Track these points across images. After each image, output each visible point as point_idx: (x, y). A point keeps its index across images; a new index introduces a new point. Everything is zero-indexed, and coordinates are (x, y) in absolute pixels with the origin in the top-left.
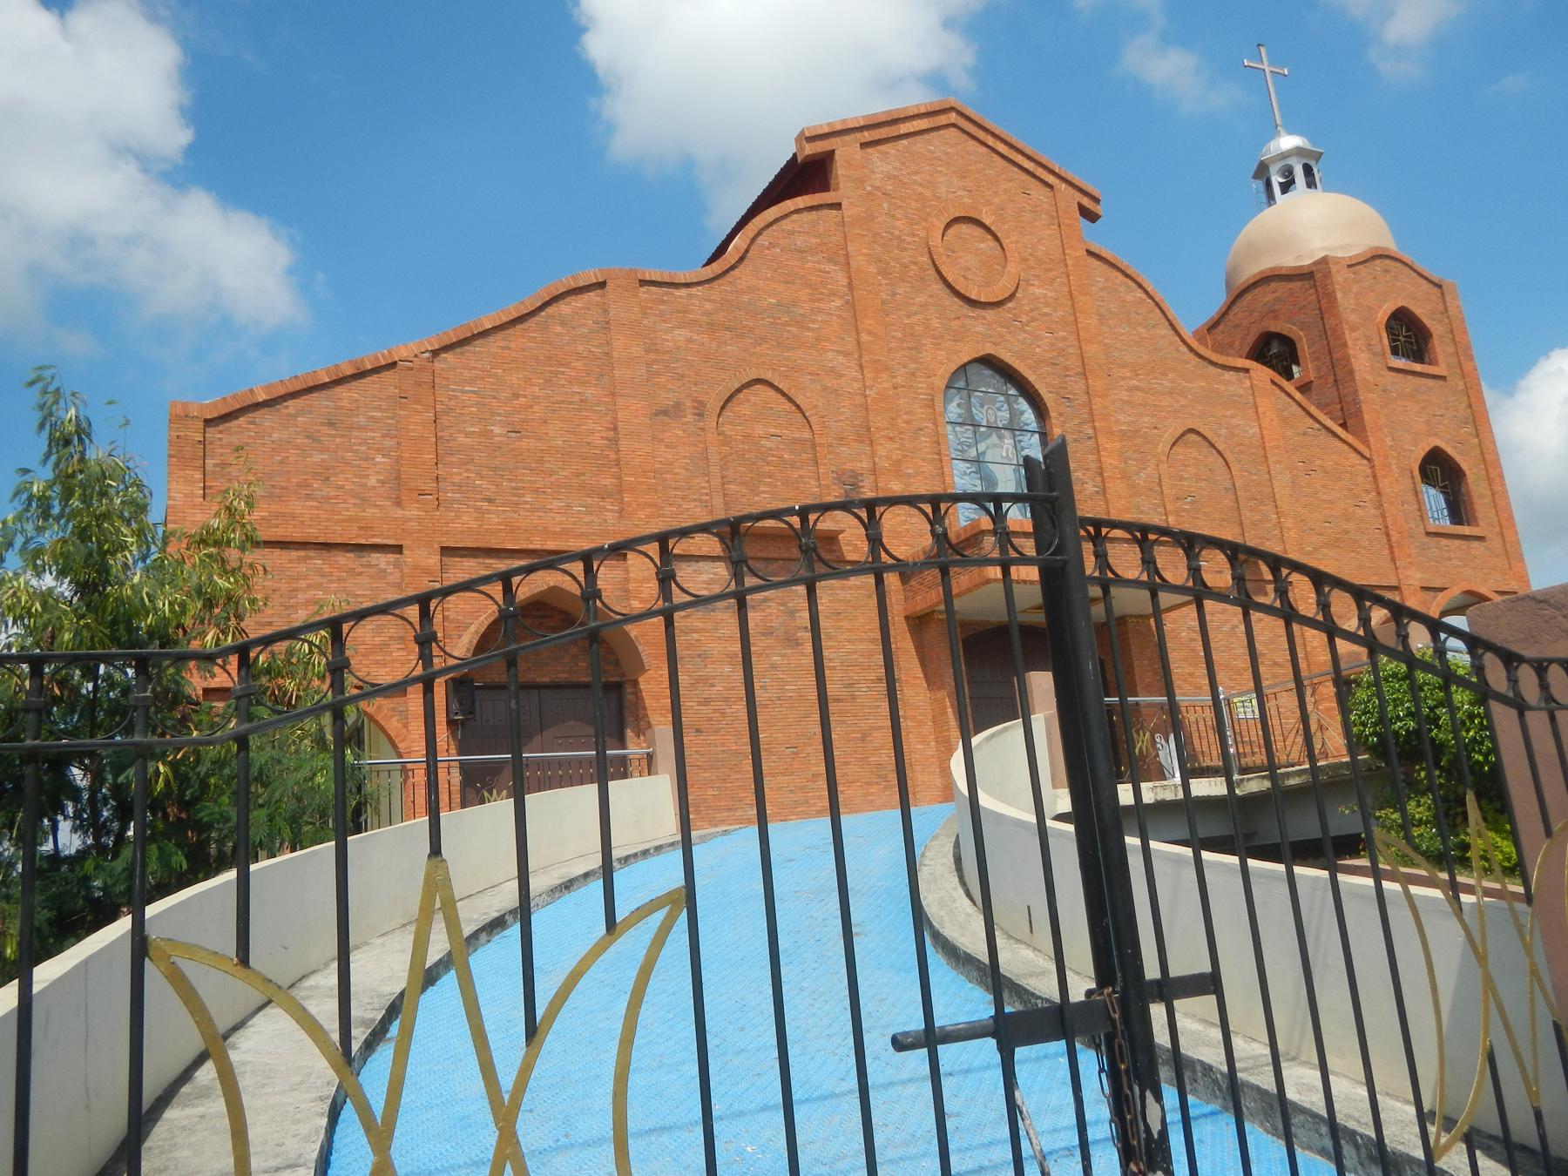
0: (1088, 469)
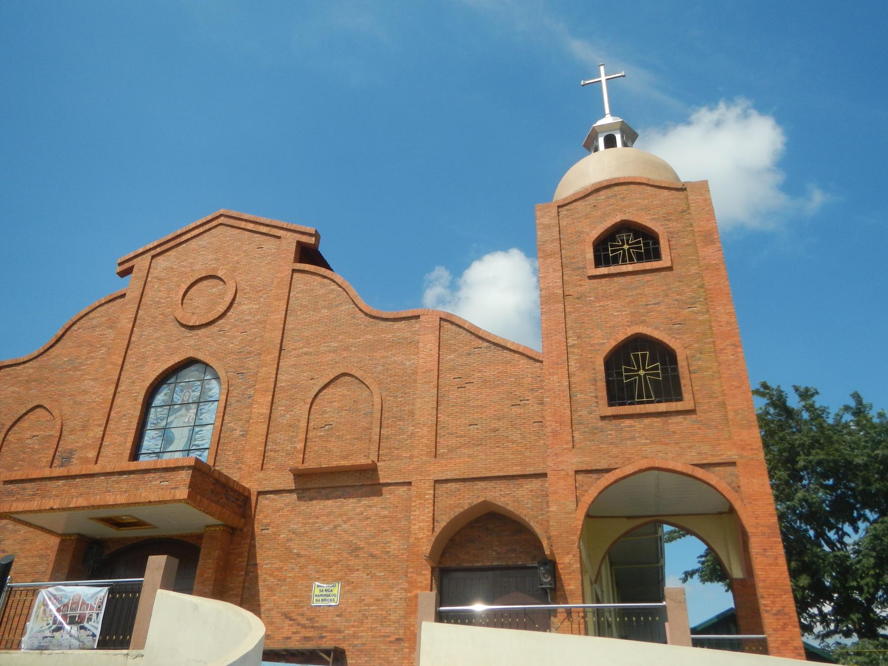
0: (241, 420)
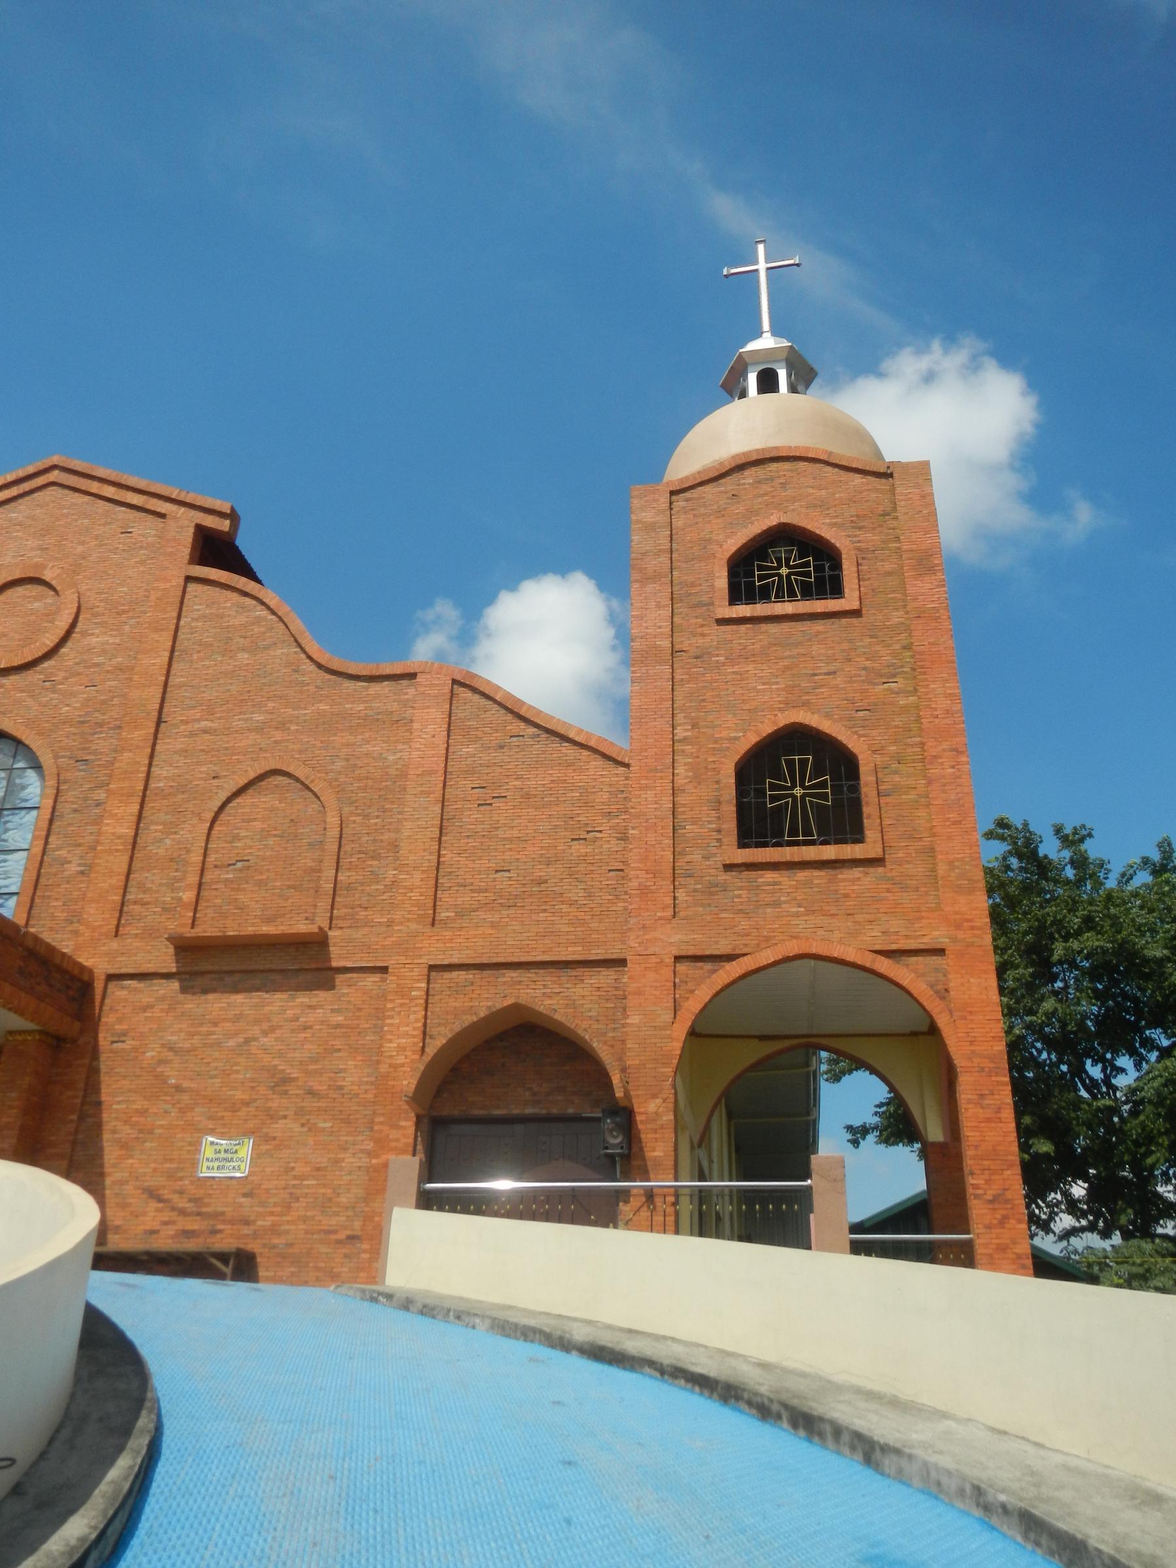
0: (80, 845)
